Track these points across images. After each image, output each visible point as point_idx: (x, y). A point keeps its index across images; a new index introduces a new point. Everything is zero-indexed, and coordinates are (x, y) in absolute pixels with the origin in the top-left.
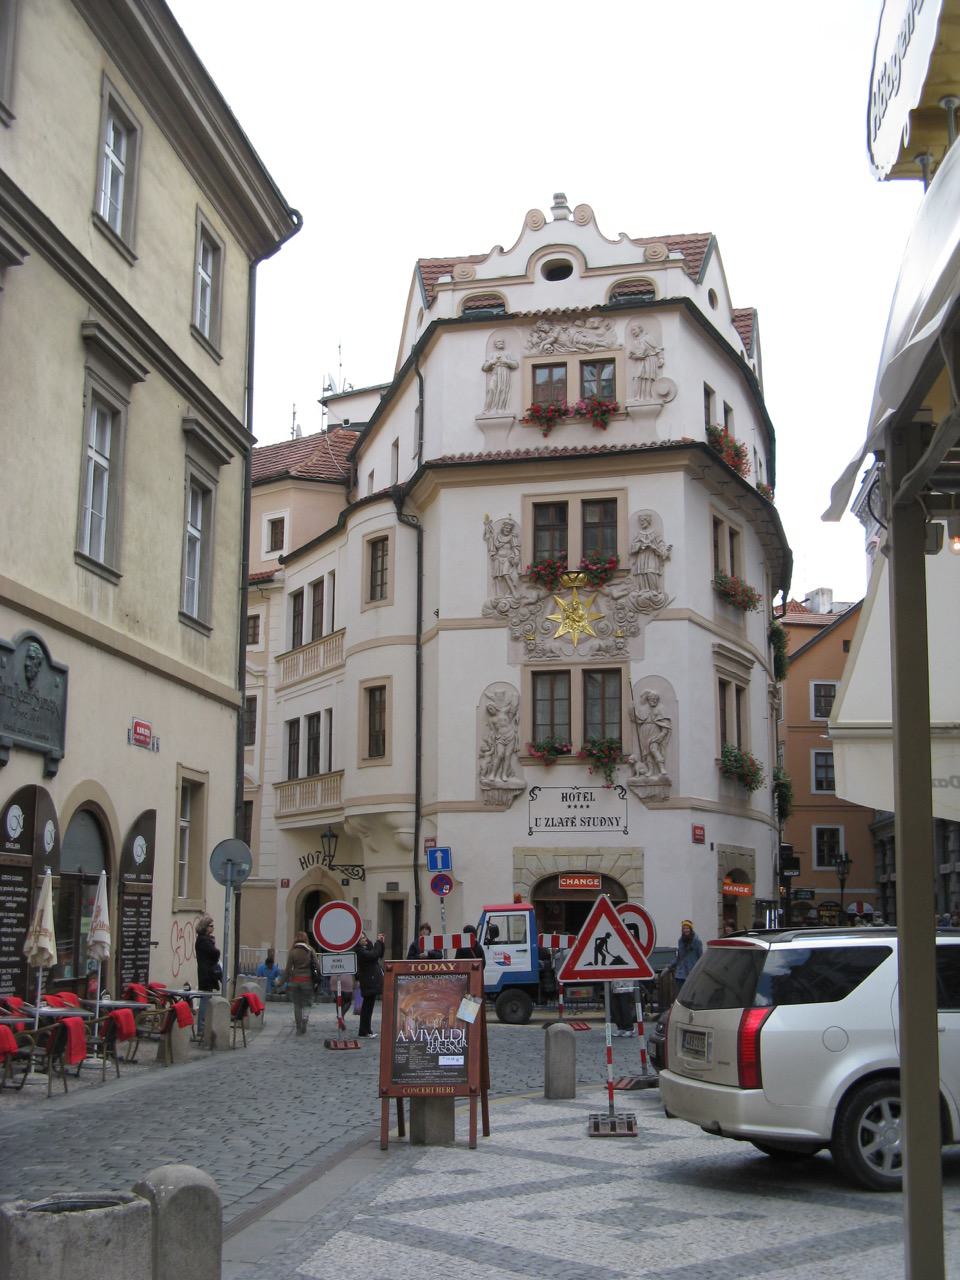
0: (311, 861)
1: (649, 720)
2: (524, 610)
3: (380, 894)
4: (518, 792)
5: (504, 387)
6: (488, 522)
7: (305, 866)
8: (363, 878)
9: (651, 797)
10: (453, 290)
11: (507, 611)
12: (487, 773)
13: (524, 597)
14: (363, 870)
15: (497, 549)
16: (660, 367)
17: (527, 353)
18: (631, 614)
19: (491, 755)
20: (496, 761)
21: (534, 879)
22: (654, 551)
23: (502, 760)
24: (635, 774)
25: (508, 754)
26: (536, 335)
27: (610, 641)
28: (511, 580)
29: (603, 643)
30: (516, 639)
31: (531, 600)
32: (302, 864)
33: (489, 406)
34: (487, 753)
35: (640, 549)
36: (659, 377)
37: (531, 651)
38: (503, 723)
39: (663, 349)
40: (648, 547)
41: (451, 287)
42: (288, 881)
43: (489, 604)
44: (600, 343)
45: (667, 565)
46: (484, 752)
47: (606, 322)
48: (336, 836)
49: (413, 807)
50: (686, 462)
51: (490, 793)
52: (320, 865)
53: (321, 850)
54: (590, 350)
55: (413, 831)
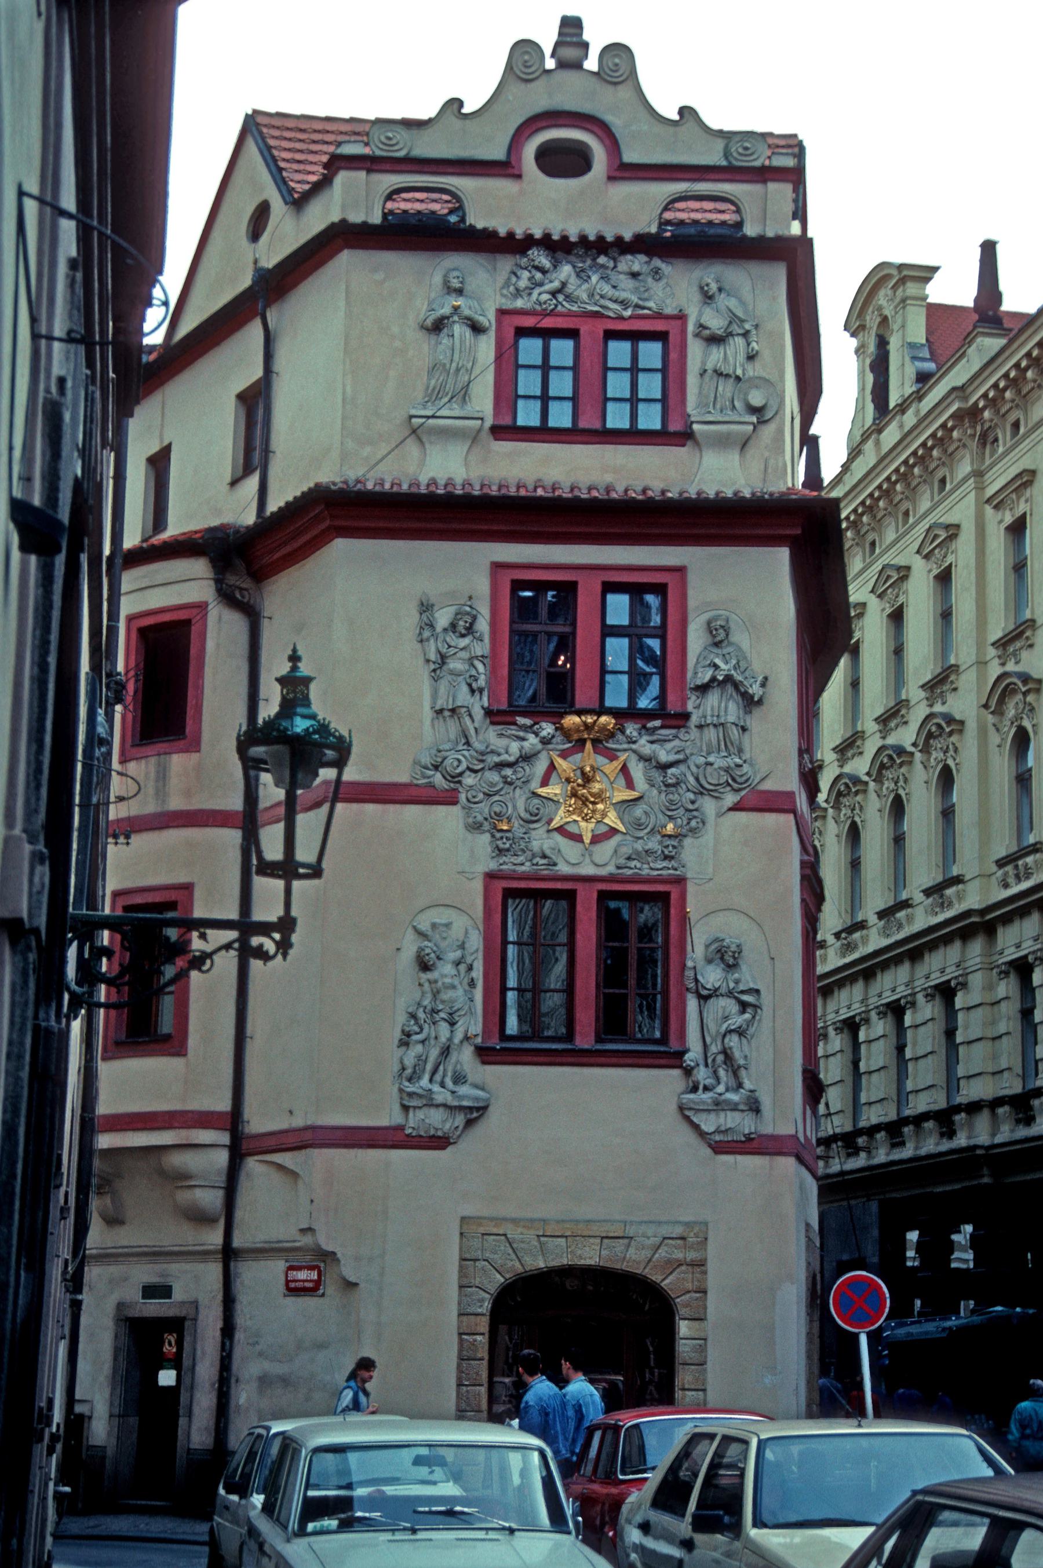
1: (723, 990)
2: (494, 777)
4: (475, 1115)
6: (426, 607)
9: (722, 1132)
10: (369, 171)
11: (461, 774)
12: (414, 1072)
13: (492, 752)
15: (443, 658)
16: (751, 357)
18: (691, 796)
19: (423, 1042)
20: (434, 1053)
21: (502, 1280)
22: (736, 685)
23: (446, 1052)
24: (694, 1089)
25: (456, 1041)
26: (526, 274)
27: (653, 844)
28: (470, 716)
29: (639, 846)
30: (475, 827)
31: (505, 757)
33: (434, 395)
34: (415, 1037)
35: (713, 679)
36: (747, 376)
37: (501, 852)
38: (448, 980)
39: (757, 326)
40: (728, 679)
43: (426, 760)
44: (641, 303)
45: (757, 712)
46: (409, 1035)
49: (225, 1138)
51: (420, 1114)
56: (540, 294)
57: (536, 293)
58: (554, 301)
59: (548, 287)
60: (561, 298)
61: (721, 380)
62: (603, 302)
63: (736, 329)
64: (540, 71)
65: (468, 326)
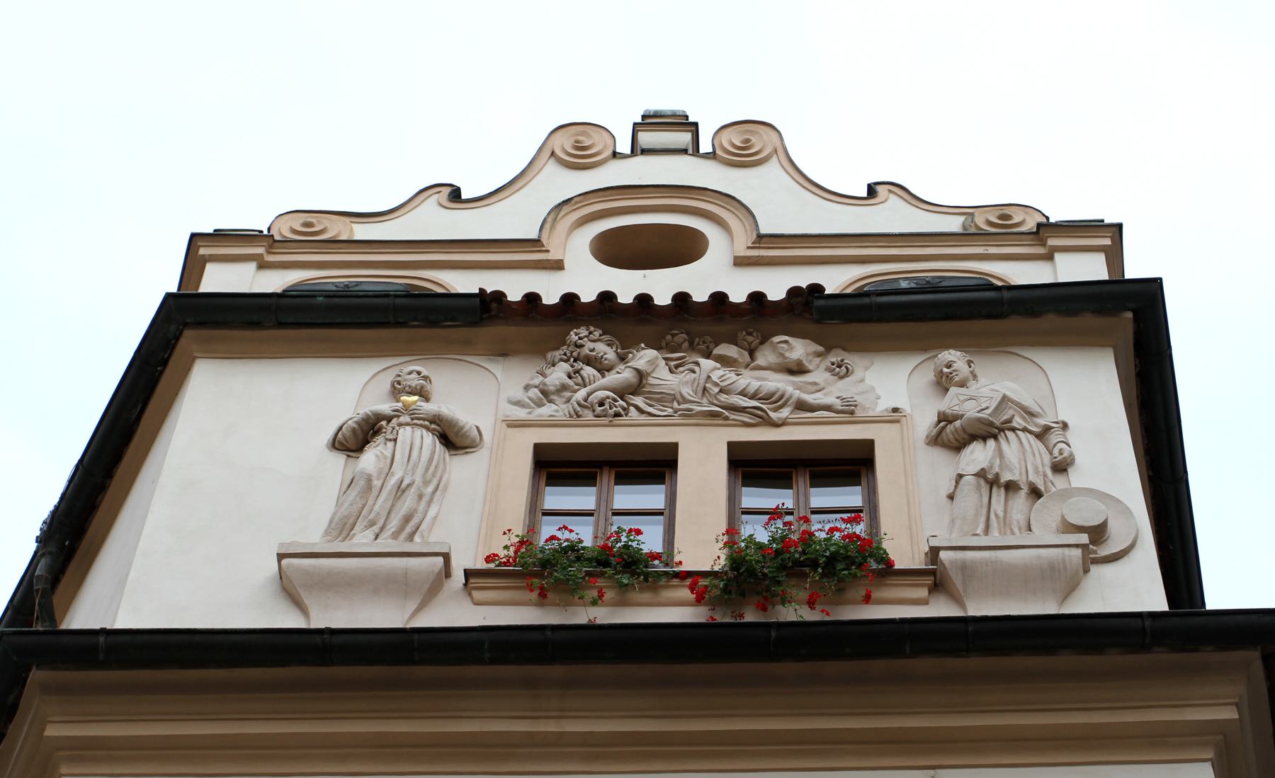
5: (418, 479)
16: (1061, 467)
17: (521, 414)
26: (564, 367)
33: (343, 527)
36: (1054, 489)
41: (260, 250)
44: (810, 398)
47: (834, 357)
50: (1230, 714)
54: (773, 415)
56: (589, 395)
57: (582, 393)
58: (621, 402)
59: (612, 378)
60: (639, 401)
61: (999, 496)
62: (723, 397)
63: (1018, 422)
64: (609, 152)
65: (432, 431)
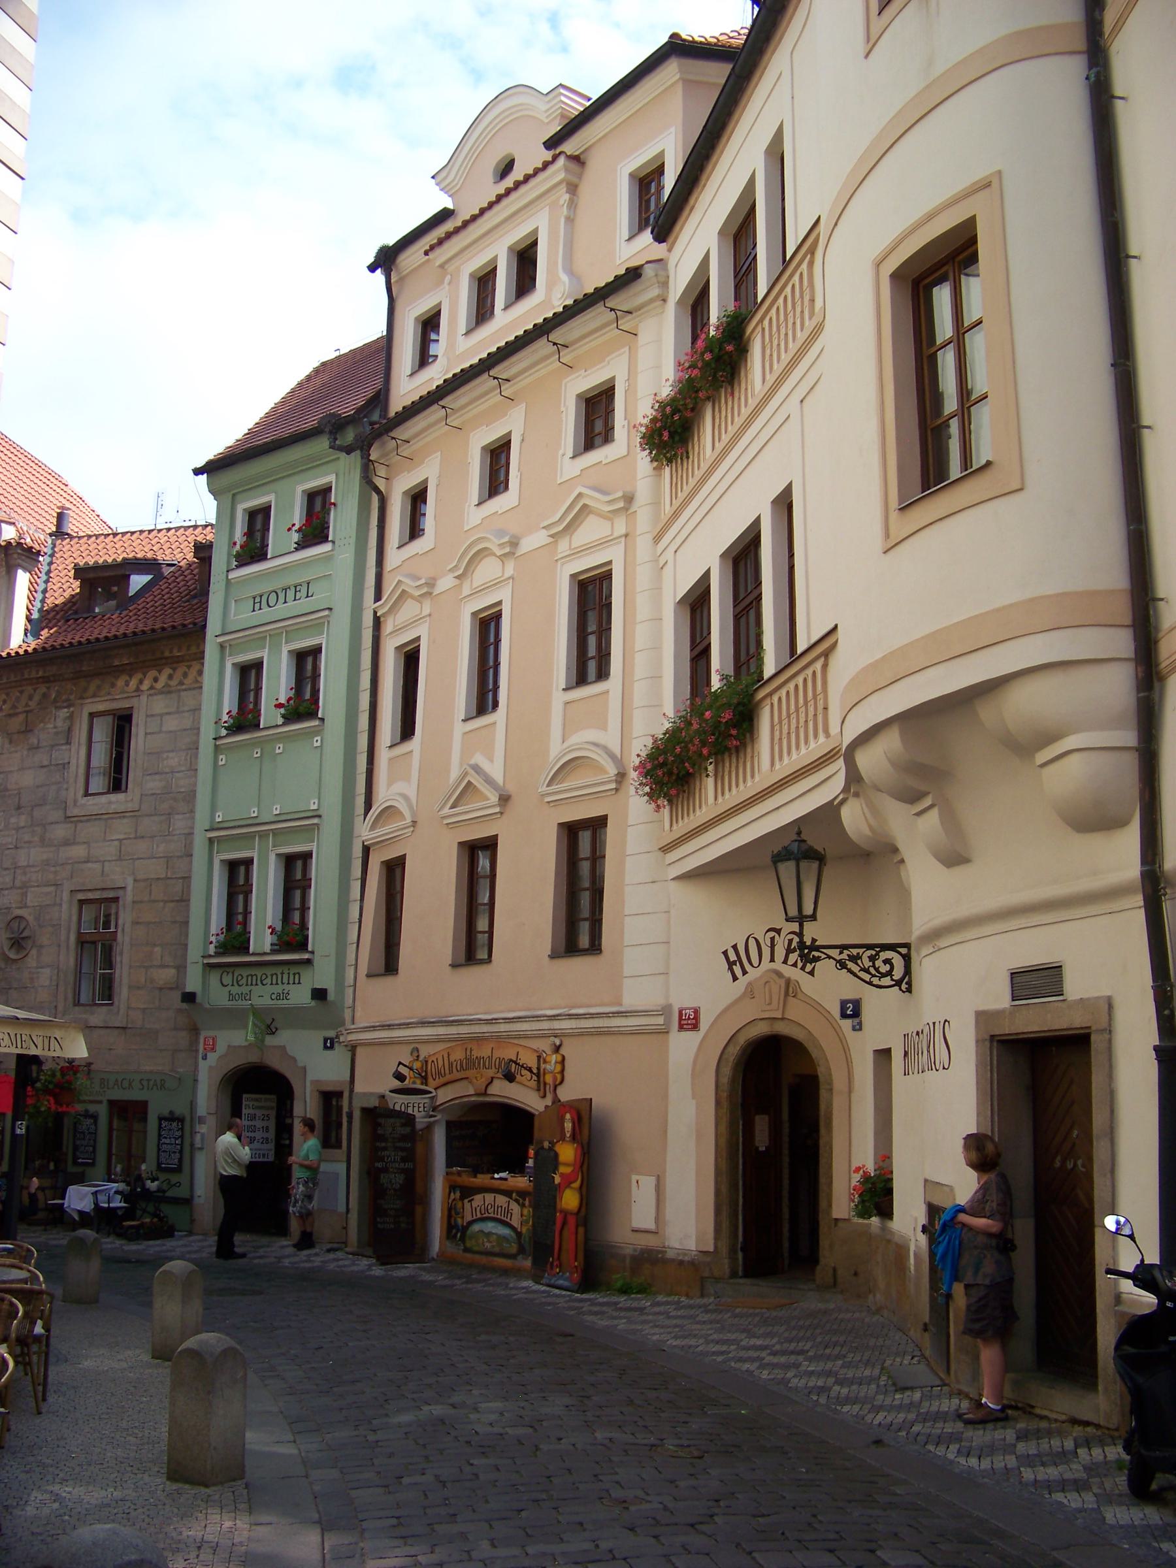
0: (755, 961)
3: (982, 1017)
7: (737, 969)
8: (906, 983)
14: (907, 959)
32: (731, 964)
42: (696, 1012)
48: (818, 857)
49: (1122, 643)
52: (778, 965)
53: (780, 922)
55: (1129, 737)
